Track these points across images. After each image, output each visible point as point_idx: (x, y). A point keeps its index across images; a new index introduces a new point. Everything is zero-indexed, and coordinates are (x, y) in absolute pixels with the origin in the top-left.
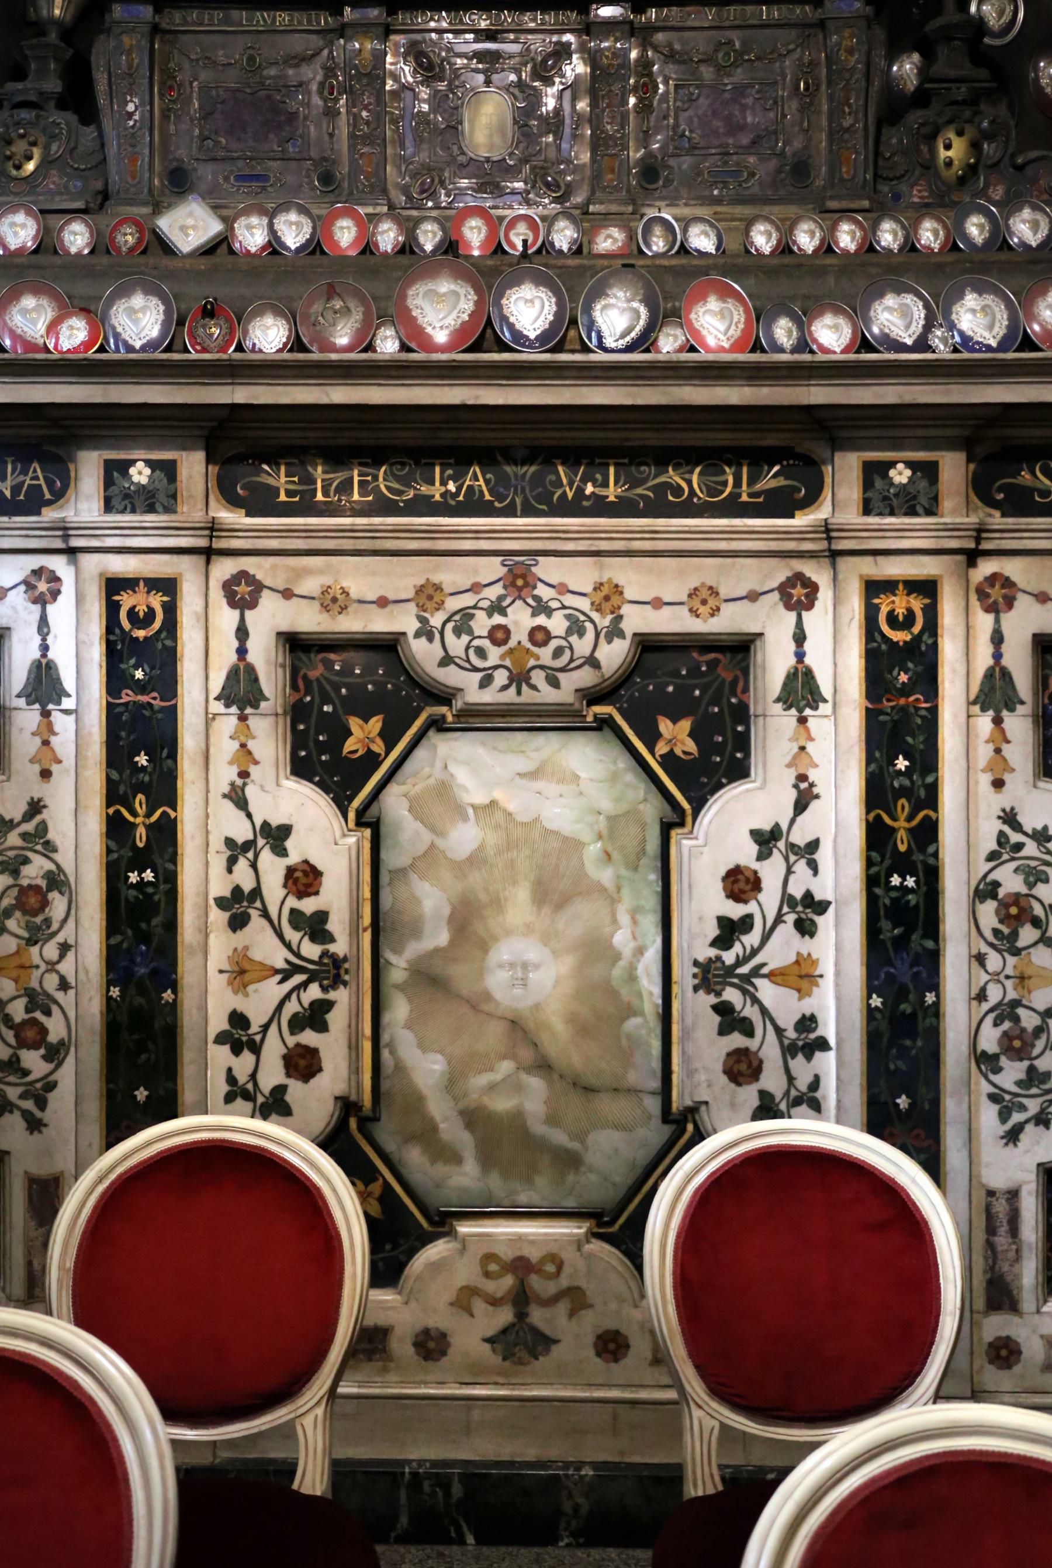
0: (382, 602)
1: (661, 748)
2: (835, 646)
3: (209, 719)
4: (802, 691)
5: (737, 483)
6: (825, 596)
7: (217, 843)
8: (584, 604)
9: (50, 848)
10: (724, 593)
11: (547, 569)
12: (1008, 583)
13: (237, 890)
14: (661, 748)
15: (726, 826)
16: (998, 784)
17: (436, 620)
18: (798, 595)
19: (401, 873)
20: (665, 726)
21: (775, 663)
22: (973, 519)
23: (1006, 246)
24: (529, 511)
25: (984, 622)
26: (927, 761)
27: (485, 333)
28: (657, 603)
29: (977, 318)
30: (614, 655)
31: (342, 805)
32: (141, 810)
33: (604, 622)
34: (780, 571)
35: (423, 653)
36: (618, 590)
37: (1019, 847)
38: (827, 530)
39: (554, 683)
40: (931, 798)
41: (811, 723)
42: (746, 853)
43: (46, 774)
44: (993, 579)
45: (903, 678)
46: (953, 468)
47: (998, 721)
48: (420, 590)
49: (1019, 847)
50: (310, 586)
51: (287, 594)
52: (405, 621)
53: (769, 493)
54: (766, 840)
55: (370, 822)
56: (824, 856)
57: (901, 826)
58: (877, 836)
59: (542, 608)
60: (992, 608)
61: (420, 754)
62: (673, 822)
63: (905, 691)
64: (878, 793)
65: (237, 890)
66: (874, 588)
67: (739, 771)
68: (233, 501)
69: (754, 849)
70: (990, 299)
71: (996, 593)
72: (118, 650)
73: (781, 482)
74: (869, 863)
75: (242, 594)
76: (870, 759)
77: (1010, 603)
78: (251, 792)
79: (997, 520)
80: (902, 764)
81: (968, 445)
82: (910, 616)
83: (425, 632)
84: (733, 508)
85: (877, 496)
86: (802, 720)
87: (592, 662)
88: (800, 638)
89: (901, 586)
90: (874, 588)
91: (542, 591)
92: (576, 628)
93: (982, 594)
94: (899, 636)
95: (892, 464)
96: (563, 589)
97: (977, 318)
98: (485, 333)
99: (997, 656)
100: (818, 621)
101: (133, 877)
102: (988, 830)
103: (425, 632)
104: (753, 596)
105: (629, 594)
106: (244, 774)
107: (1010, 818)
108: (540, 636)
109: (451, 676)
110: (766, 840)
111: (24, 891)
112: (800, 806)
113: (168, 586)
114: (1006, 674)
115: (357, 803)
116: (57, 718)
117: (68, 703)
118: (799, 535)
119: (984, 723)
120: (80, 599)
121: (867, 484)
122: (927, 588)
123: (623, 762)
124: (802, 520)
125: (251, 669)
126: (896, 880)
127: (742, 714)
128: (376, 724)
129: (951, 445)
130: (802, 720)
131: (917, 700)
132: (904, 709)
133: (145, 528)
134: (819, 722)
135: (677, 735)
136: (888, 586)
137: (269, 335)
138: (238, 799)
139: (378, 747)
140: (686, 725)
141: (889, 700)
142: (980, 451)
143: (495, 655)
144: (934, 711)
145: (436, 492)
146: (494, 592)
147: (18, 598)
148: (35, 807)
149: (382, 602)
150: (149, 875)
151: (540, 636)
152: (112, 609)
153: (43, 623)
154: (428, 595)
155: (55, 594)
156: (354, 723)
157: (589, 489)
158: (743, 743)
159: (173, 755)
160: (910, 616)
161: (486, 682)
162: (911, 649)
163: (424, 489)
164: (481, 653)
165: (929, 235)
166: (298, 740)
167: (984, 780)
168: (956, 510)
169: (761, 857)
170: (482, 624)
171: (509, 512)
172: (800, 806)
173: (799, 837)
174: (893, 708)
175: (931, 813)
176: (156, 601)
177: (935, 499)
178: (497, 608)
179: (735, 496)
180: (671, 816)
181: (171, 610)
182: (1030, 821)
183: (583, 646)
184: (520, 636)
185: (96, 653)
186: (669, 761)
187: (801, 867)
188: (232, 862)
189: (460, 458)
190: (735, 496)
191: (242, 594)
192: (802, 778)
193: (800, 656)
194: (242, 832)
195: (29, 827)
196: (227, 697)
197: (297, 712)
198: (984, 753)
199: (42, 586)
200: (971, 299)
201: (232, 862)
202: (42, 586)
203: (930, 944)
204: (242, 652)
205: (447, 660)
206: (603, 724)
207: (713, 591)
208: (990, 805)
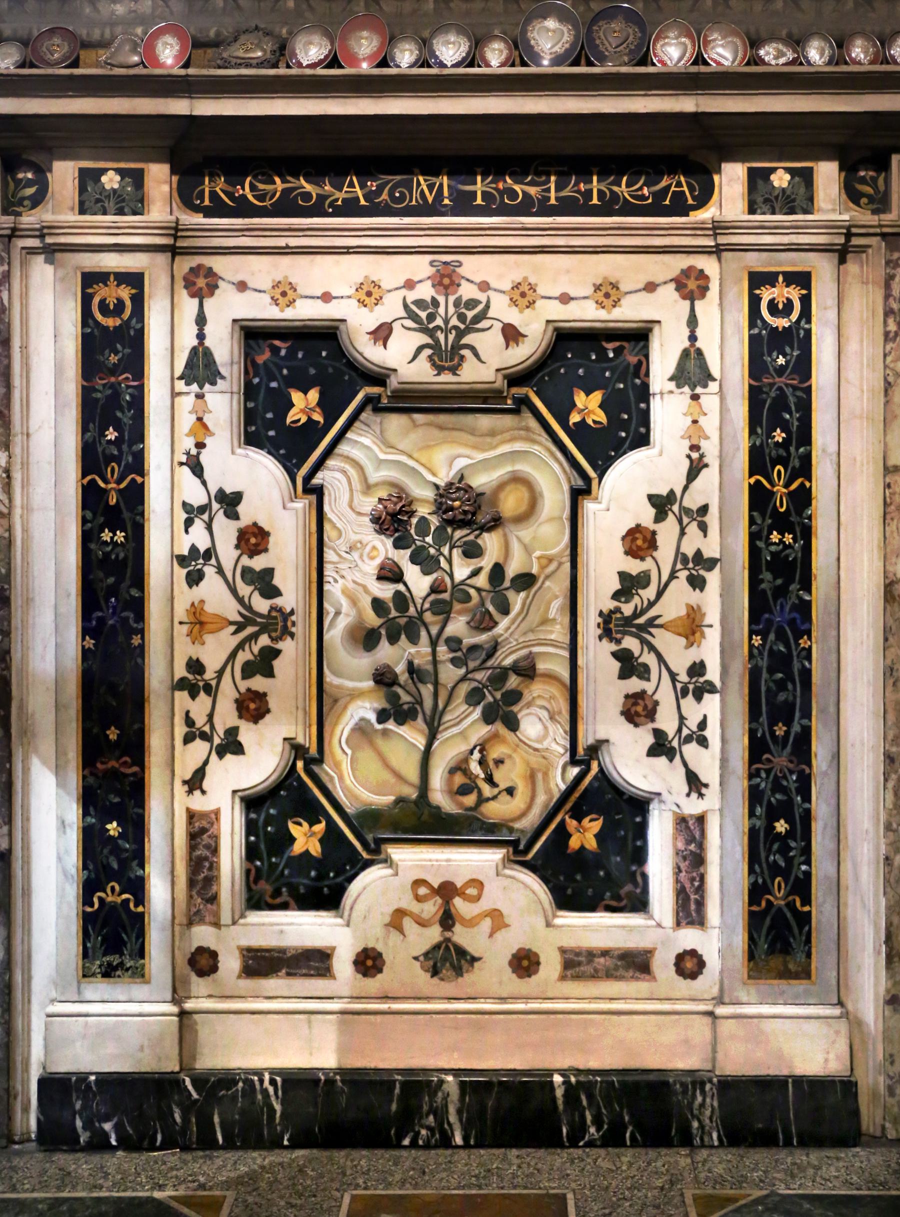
22: (173, 218)
45: (114, 359)
64: (92, 459)
74: (84, 521)
79: (198, 219)
80: (111, 435)
89: (112, 278)
94: (111, 322)
95: (104, 171)
121: (82, 189)
122: (135, 280)
131: (127, 378)
141: (100, 379)
144: (141, 388)
160: (120, 304)
174: (104, 385)
175: (139, 479)
203: (135, 593)
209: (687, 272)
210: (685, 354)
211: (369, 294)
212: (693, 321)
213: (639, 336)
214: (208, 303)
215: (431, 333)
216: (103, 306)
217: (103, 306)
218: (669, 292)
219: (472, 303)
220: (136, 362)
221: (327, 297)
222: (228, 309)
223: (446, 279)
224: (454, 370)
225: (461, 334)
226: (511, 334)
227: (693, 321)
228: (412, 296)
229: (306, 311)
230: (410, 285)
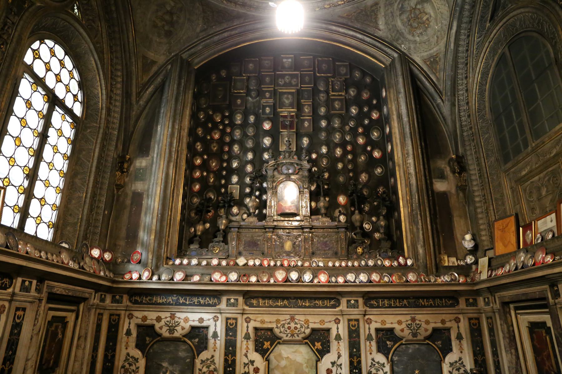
0: (270, 322)
1: (316, 348)
2: (342, 329)
3: (242, 342)
4: (338, 338)
6: (341, 322)
7: (242, 363)
8: (303, 323)
9: (215, 364)
10: (326, 321)
11: (297, 317)
12: (371, 319)
13: (245, 372)
14: (316, 348)
15: (326, 362)
16: (371, 354)
17: (279, 325)
18: (337, 321)
19: (273, 369)
20: (316, 343)
21: (334, 333)
22: (364, 309)
23: (367, 266)
24: (294, 307)
25: (367, 326)
26: (359, 350)
27: (287, 280)
28: (315, 323)
29: (363, 277)
30: (308, 331)
31: (263, 357)
32: (230, 357)
33: (306, 326)
34: (334, 318)
35: (277, 331)
36: (308, 320)
37: (375, 365)
38: (341, 311)
39: (298, 336)
40: (360, 356)
41: (340, 343)
42: (330, 366)
43: (215, 351)
44: (368, 319)
46: (361, 301)
47: (370, 343)
48: (276, 320)
49: (375, 365)
50: (259, 319)
51: (255, 321)
52: (274, 325)
53: (332, 305)
54: (333, 364)
55: (268, 360)
56: (343, 366)
57: (355, 361)
58: (351, 363)
59: (296, 323)
60: (368, 324)
61: (276, 348)
62: (318, 360)
63: (355, 338)
64: (351, 355)
65: (245, 372)
66: (349, 320)
67: (329, 352)
68: (247, 305)
69: (331, 365)
70: (365, 275)
71: (369, 321)
72: (228, 330)
74: (350, 368)
75: (248, 321)
76: (350, 349)
77: (371, 323)
78: (248, 355)
79: (368, 309)
80: (355, 350)
81: (363, 297)
82: (355, 325)
83: (277, 327)
84: (326, 307)
85: (349, 305)
86: (338, 343)
87: (304, 333)
88: (338, 329)
90: (349, 320)
91: (296, 321)
92: (302, 327)
93: (366, 321)
96: (299, 320)
97: (363, 277)
99: (369, 332)
100: (340, 326)
101: (228, 369)
102: (370, 361)
103: (277, 327)
104: (330, 322)
105: (310, 321)
106: (247, 351)
107: (373, 360)
108: (296, 328)
109: (281, 335)
110: (333, 364)
111: (210, 371)
112: (339, 358)
113: (236, 319)
114: (371, 335)
115: (266, 357)
116: (217, 341)
117: (219, 338)
118: (337, 312)
119: (368, 343)
120: (222, 321)
121: (347, 303)
122: (358, 320)
123: (310, 350)
124: (337, 309)
125: (249, 333)
126: (354, 371)
127: (329, 341)
128: (269, 343)
129: (360, 297)
130: (338, 343)
132: (355, 341)
133: (232, 309)
134: (341, 343)
135: (318, 345)
136: (351, 320)
137: (253, 279)
138: (246, 356)
139: (269, 347)
140: (320, 343)
142: (365, 298)
143: (288, 331)
144: (359, 341)
145: (279, 304)
146: (288, 321)
147: (212, 320)
148: (213, 356)
149: (270, 322)
150: (231, 369)
151: (296, 328)
152: (227, 323)
153: (216, 325)
154: (278, 321)
155: (218, 320)
156: (265, 343)
158: (329, 346)
159: (236, 348)
160: (355, 325)
161: (287, 336)
162: (355, 330)
164: (286, 331)
165: (356, 264)
166: (256, 346)
167: (368, 353)
168: (361, 307)
169: (332, 367)
170: (286, 326)
171: (291, 307)
172: (339, 358)
173: (339, 363)
176: (234, 321)
178: (289, 323)
180: (317, 359)
181: (236, 323)
182: (376, 360)
183: (303, 330)
184: (292, 328)
185: (224, 330)
186: (317, 350)
187: (339, 368)
188: (245, 367)
189: (283, 299)
191: (248, 321)
192: (339, 353)
193: (338, 332)
194: (246, 361)
195: (211, 360)
196: (245, 338)
197: (256, 341)
198: (368, 348)
199: (216, 319)
200: (362, 274)
201: (245, 367)
202: (216, 319)
204: (247, 330)
205: (281, 332)
206: (306, 343)
207: (324, 321)
208: (370, 357)
209: (457, 318)
210: (458, 333)
211: (400, 323)
212: (458, 327)
213: (448, 330)
214: (371, 325)
215: (411, 330)
216: (352, 325)
217: (352, 325)
218: (453, 322)
219: (418, 324)
220: (358, 336)
221: (392, 323)
222: (374, 326)
223: (413, 320)
224: (416, 337)
225: (417, 330)
226: (426, 330)
227: (458, 327)
228: (407, 323)
229: (388, 326)
230: (407, 321)
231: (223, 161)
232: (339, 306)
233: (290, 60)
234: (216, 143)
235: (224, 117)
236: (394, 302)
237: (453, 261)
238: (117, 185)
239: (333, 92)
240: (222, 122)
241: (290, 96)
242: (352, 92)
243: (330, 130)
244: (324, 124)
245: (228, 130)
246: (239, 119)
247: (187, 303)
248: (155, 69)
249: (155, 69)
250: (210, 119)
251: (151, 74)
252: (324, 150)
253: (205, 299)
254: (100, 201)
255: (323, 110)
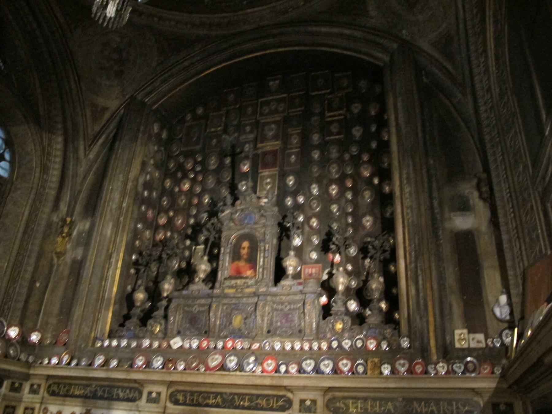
5: (273, 403)
24: (229, 407)
27: (222, 367)
68: (171, 402)
73: (282, 403)
84: (272, 409)
98: (222, 367)
121: (300, 405)
137: (181, 367)
145: (211, 402)
157: (242, 403)
163: (208, 401)
171: (225, 407)
177: (316, 409)
179: (272, 406)
190: (272, 406)
231: (189, 216)
232: (288, 409)
233: (277, 82)
234: (185, 195)
235: (196, 163)
236: (371, 406)
237: (478, 340)
238: (57, 253)
239: (329, 111)
240: (193, 169)
241: (273, 126)
242: (356, 108)
243: (325, 162)
244: (316, 155)
245: (200, 178)
246: (213, 163)
247: (106, 396)
248: (107, 115)
249: (107, 115)
250: (180, 167)
251: (103, 123)
252: (315, 191)
253: (125, 392)
254: (26, 271)
255: (316, 138)
